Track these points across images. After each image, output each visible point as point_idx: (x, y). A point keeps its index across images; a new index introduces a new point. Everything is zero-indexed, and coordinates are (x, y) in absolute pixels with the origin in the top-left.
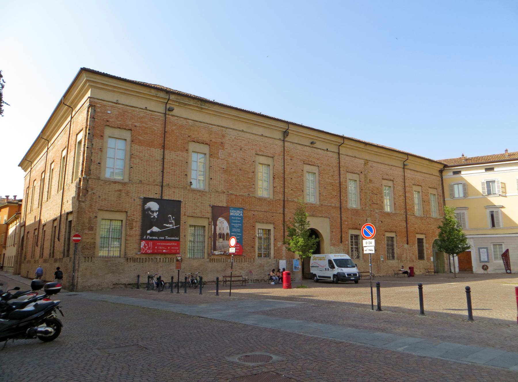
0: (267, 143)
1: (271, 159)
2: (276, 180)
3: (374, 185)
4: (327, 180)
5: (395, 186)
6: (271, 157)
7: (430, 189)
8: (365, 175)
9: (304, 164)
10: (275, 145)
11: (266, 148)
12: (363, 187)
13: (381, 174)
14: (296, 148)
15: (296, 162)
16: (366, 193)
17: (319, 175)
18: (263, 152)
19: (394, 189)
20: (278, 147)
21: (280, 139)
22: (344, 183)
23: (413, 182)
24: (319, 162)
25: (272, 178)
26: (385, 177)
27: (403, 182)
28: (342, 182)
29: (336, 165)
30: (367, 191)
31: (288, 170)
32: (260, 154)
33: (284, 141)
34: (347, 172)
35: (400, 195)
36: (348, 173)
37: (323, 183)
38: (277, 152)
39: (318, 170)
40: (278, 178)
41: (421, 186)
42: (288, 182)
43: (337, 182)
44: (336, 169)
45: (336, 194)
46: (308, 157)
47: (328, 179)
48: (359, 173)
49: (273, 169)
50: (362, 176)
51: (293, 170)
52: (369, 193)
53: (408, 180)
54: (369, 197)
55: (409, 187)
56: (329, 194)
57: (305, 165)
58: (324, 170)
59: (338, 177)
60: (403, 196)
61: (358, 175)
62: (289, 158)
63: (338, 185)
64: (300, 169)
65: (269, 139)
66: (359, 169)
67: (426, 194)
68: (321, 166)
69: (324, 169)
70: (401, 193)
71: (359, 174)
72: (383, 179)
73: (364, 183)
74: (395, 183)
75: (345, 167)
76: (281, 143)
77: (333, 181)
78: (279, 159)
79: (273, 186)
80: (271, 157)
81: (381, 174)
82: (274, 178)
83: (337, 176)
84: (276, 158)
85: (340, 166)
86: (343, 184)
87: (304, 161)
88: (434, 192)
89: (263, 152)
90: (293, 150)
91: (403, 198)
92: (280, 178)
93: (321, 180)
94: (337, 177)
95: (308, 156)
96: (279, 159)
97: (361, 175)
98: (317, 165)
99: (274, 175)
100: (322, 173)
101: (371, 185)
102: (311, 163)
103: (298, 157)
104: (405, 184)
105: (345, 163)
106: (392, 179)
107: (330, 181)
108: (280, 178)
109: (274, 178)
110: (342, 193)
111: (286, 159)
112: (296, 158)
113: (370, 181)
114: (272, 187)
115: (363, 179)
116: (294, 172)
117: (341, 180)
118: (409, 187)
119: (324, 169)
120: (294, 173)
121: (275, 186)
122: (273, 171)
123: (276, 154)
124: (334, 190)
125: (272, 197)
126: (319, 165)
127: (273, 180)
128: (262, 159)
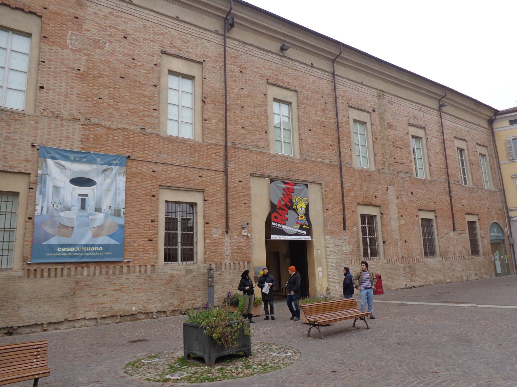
0: (188, 35)
1: (198, 66)
2: (209, 107)
3: (396, 133)
4: (314, 117)
5: (428, 136)
6: (198, 62)
7: (478, 147)
8: (380, 114)
9: (268, 83)
10: (206, 41)
11: (185, 42)
12: (378, 134)
13: (406, 117)
14: (251, 53)
15: (251, 78)
16: (383, 144)
17: (298, 106)
18: (180, 50)
19: (427, 142)
20: (212, 45)
21: (216, 32)
22: (344, 125)
23: (454, 133)
24: (297, 83)
25: (199, 104)
26: (412, 122)
27: (440, 133)
28: (342, 123)
29: (328, 92)
30: (385, 142)
31: (235, 91)
32: (173, 53)
33: (224, 35)
34: (350, 107)
35: (437, 151)
36: (350, 109)
37: (306, 120)
38: (210, 55)
39: (295, 98)
40: (213, 102)
41: (465, 140)
42: (235, 113)
43: (332, 121)
44: (330, 100)
45: (330, 142)
46: (276, 73)
47: (316, 114)
48: (371, 111)
49: (203, 85)
50: (375, 115)
51: (245, 92)
52: (388, 144)
53: (448, 129)
54: (389, 152)
55: (450, 141)
56: (318, 141)
57: (270, 87)
58: (307, 98)
59: (332, 113)
60: (442, 154)
61: (368, 115)
62: (237, 70)
63: (334, 127)
64: (260, 91)
65: (192, 27)
66: (369, 105)
67: (474, 153)
68: (301, 92)
69: (307, 96)
70: (439, 148)
71: (369, 112)
72: (410, 125)
73: (379, 128)
74: (427, 131)
75: (345, 98)
76: (219, 39)
77: (324, 120)
78: (215, 68)
79: (203, 118)
80: (198, 62)
81: (406, 117)
82: (204, 102)
83: (331, 111)
84: (208, 65)
85: (337, 96)
86: (343, 127)
87: (268, 78)
88: (484, 151)
89: (180, 50)
90: (244, 56)
91: (441, 156)
92: (217, 104)
93: (303, 116)
94: (331, 114)
95: (275, 70)
96: (215, 68)
97: (373, 114)
98: (293, 88)
99: (204, 96)
100: (304, 104)
101: (392, 132)
102: (281, 84)
103: (256, 70)
104: (443, 135)
105: (345, 91)
106: (424, 126)
107: (319, 118)
108: (217, 104)
109: (204, 102)
110: (342, 142)
111: (230, 70)
112: (252, 71)
113: (390, 126)
114: (201, 118)
115: (377, 121)
116: (249, 96)
117: (339, 119)
118: (450, 141)
119: (307, 96)
120: (247, 96)
121: (206, 117)
122: (202, 88)
123: (207, 57)
124: (328, 135)
125: (199, 139)
126: (297, 89)
127: (202, 106)
128: (177, 65)
